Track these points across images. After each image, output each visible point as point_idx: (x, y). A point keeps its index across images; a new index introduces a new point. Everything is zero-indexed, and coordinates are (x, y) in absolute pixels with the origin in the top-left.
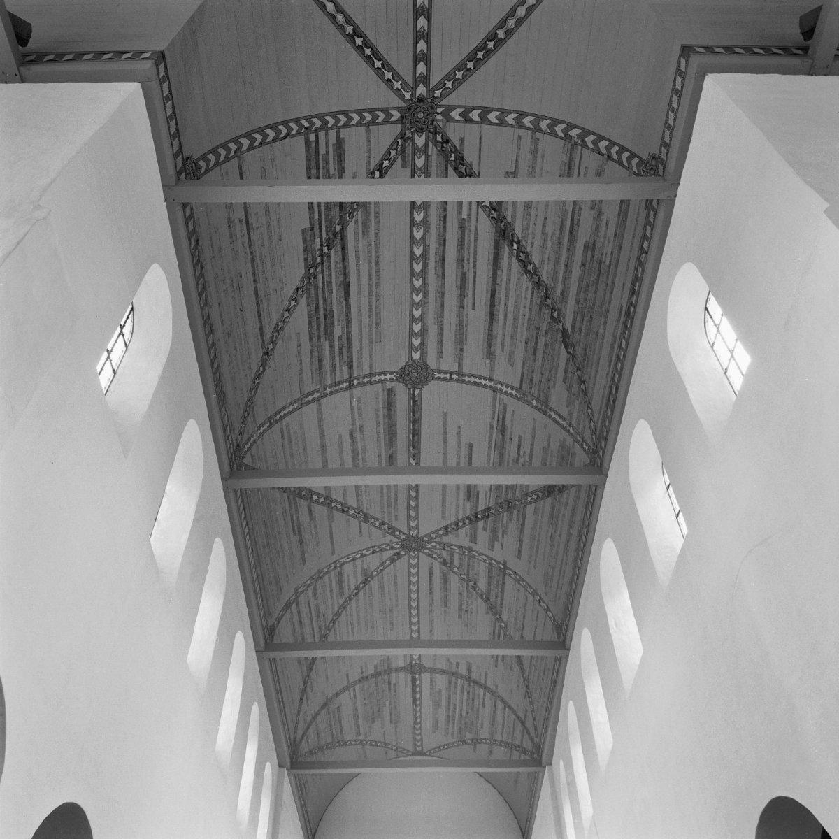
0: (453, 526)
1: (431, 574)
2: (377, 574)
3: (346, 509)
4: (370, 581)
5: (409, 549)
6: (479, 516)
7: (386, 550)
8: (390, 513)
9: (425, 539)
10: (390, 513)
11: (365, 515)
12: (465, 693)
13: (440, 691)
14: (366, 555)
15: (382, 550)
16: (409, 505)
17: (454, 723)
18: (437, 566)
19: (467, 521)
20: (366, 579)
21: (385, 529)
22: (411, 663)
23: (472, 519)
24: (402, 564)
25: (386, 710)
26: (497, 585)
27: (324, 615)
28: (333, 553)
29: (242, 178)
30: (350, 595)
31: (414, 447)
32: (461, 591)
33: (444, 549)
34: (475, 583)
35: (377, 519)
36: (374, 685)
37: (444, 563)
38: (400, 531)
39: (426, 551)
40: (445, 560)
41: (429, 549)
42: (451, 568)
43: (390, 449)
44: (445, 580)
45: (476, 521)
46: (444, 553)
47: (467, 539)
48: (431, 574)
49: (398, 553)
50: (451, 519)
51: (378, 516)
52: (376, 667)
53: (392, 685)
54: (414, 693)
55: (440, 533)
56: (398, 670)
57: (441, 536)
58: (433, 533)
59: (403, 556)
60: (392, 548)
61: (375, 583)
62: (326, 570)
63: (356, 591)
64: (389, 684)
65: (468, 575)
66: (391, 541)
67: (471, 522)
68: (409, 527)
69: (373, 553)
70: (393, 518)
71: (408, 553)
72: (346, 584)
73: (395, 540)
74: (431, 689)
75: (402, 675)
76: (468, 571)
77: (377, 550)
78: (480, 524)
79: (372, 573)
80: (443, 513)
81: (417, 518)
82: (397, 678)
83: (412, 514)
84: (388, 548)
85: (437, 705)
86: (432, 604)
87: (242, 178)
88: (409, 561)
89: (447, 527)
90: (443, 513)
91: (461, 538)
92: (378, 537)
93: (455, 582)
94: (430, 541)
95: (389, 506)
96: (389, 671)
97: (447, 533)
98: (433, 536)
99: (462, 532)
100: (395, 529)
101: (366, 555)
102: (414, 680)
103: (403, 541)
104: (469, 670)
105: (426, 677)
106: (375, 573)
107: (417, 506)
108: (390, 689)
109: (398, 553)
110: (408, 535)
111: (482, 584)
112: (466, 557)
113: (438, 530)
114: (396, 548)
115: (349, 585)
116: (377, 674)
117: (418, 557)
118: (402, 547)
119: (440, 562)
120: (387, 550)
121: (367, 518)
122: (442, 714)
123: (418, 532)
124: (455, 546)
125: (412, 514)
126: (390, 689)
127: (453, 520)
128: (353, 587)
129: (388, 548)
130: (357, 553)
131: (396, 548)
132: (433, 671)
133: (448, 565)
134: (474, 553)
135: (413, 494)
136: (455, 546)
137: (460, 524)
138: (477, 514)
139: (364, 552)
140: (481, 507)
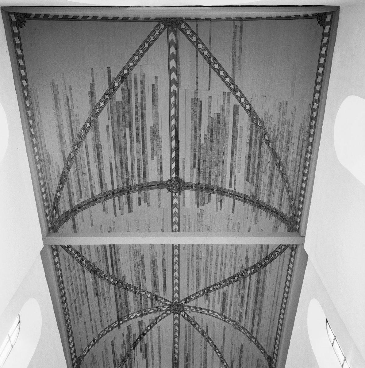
0: (153, 325)
1: (165, 286)
2: (200, 291)
3: (213, 346)
4: (205, 289)
5: (179, 304)
6: (139, 340)
7: (193, 307)
8: (190, 330)
9: (169, 312)
10: (190, 330)
11: (203, 335)
12: (130, 170)
13: (153, 158)
14: (206, 310)
15: (196, 308)
16: (179, 334)
17: (137, 107)
18: (161, 294)
19: (145, 332)
20: (208, 292)
21: (193, 321)
22: (179, 194)
23: (143, 334)
24: (184, 295)
25: (204, 131)
26: (121, 305)
27: (239, 293)
28: (225, 294)
29: (249, 231)
30: (220, 287)
31: (176, 363)
32: (144, 280)
33: (157, 307)
34: (135, 293)
35: (197, 329)
36: (213, 177)
37: (157, 297)
38: (184, 317)
39: (168, 303)
40: (156, 299)
41: (167, 305)
42: (152, 295)
43: (188, 364)
44: (155, 284)
45: (140, 336)
46: (157, 304)
47: (144, 321)
48: (165, 286)
49: (186, 302)
50: (155, 329)
51: (195, 330)
52: (209, 199)
53: (197, 166)
54: (177, 149)
55: (160, 318)
56: (190, 187)
57: (160, 316)
58: (165, 317)
59: (183, 300)
60: (190, 307)
61: (202, 287)
62: (231, 323)
63: (215, 287)
64: (199, 169)
65: (141, 296)
66: (190, 312)
67: (143, 332)
68: (179, 320)
69: (201, 309)
70: (188, 327)
71: (180, 302)
72: (221, 299)
73: (188, 312)
74: (161, 157)
75: (187, 180)
76: (141, 299)
77: (198, 309)
78: (137, 336)
79: (203, 295)
80: (159, 330)
81: (174, 325)
82: (192, 175)
83: (177, 328)
84: (192, 308)
85: (155, 132)
86: (164, 260)
87: (249, 231)
88: (179, 296)
89: (157, 323)
90: (159, 330)
91: (147, 320)
92: (197, 317)
93: (149, 286)
94: (166, 310)
95: (190, 334)
96: (198, 188)
97: (156, 319)
98: (165, 315)
99: (147, 324)
100: (187, 319)
101: (206, 310)
102: (177, 169)
103: (183, 311)
104: (129, 203)
105: (166, 176)
106: (202, 293)
107: (174, 333)
108: (199, 161)
109: (186, 302)
110: (179, 314)
111: (131, 295)
112: (143, 309)
113: (162, 319)
114: (187, 306)
115: (219, 296)
116: (209, 189)
117: (174, 299)
118: (183, 306)
119: (159, 297)
120: (193, 307)
121: (203, 333)
122: (149, 123)
123: (173, 316)
124: (151, 313)
125: (177, 328)
126: (199, 161)
127: (153, 329)
128: (217, 291)
129: (192, 308)
130: (210, 315)
131: (187, 306)
132: (160, 185)
133: (154, 297)
134: (138, 315)
135: (176, 340)
136: (151, 313)
137: (149, 328)
138: (140, 340)
139: (207, 313)
140: (138, 346)
